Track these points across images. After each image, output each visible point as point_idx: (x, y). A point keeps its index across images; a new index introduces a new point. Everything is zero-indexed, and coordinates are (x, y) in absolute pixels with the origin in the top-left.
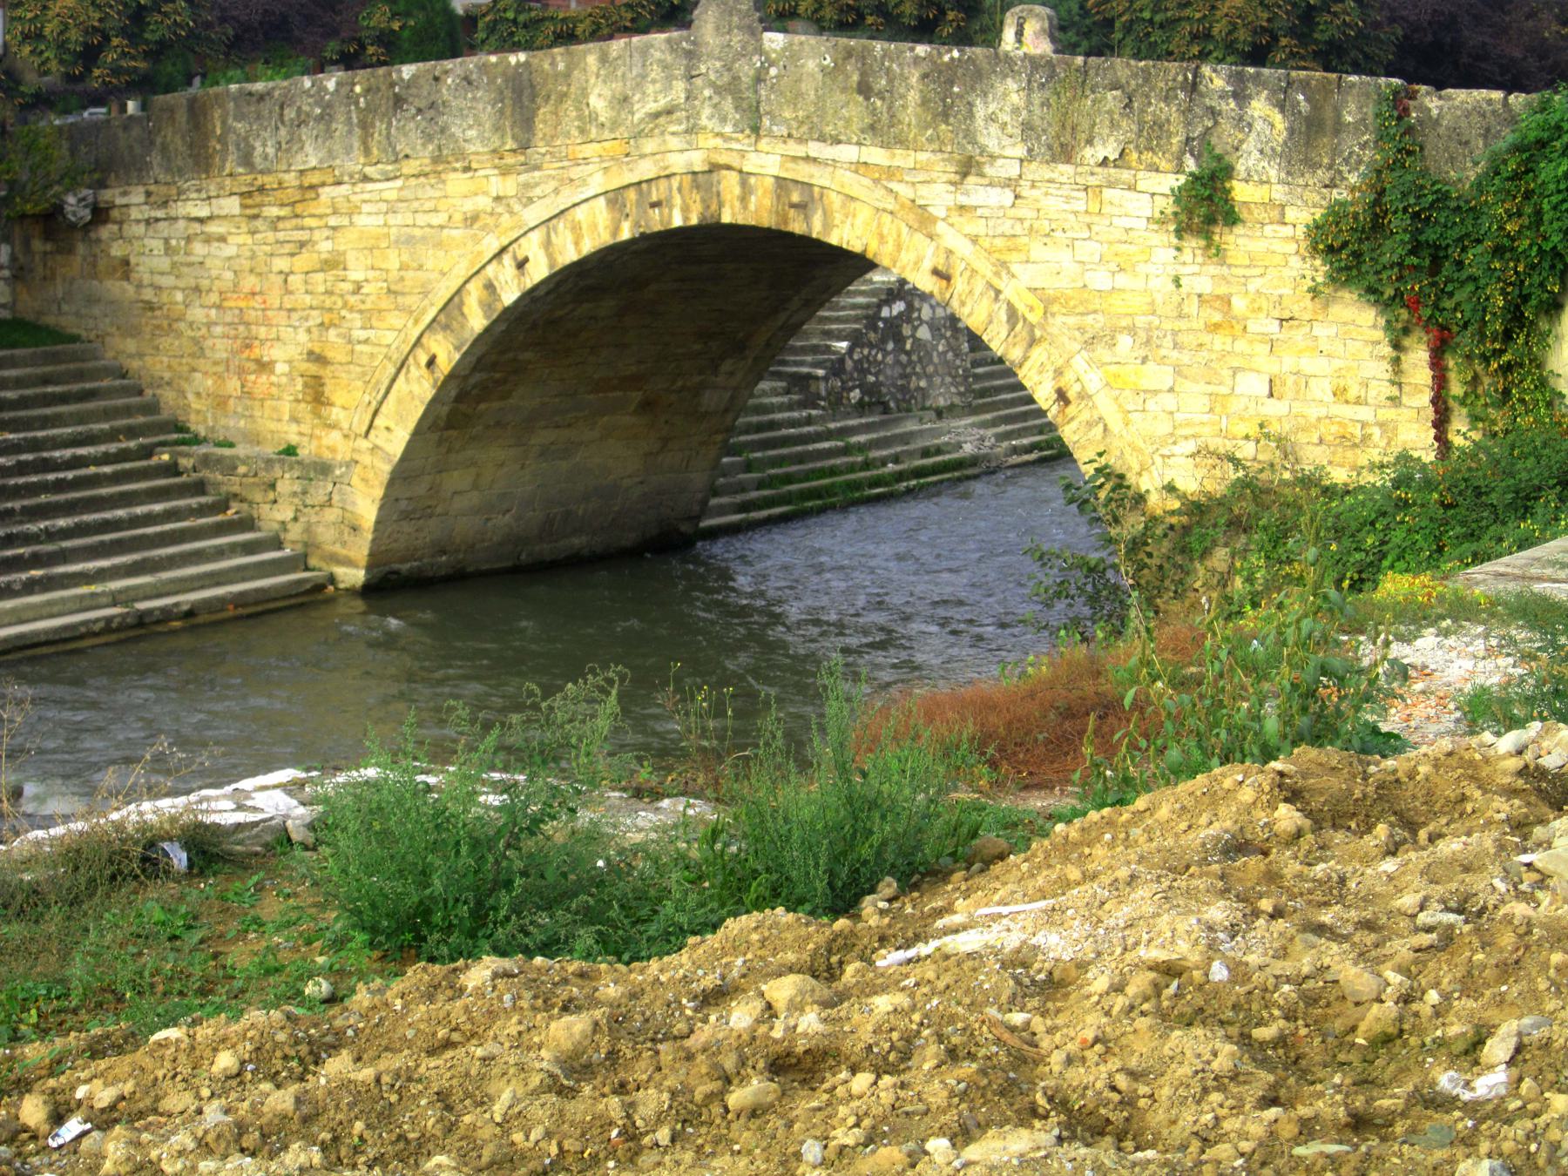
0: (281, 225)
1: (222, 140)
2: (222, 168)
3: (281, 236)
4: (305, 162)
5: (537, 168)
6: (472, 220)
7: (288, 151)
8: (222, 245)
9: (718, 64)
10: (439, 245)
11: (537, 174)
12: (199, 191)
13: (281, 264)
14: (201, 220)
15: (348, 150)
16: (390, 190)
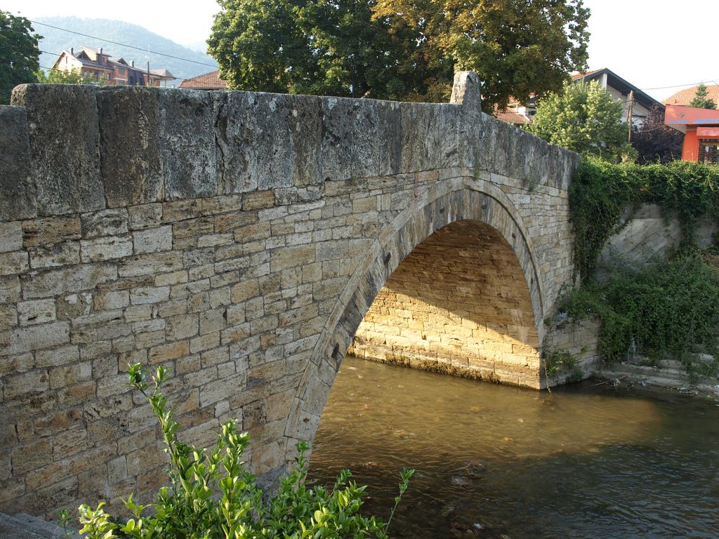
0: (219, 254)
1: (149, 155)
2: (148, 193)
3: (220, 266)
4: (247, 184)
5: (402, 189)
6: (364, 229)
7: (231, 172)
8: (149, 289)
9: (470, 126)
10: (348, 254)
11: (400, 193)
12: (117, 224)
13: (219, 297)
14: (119, 263)
15: (286, 170)
16: (316, 209)
